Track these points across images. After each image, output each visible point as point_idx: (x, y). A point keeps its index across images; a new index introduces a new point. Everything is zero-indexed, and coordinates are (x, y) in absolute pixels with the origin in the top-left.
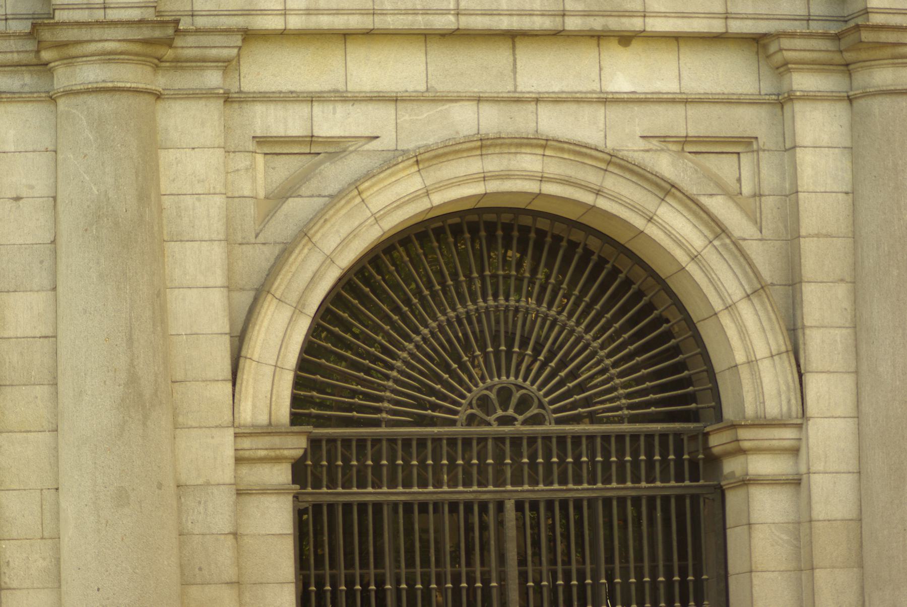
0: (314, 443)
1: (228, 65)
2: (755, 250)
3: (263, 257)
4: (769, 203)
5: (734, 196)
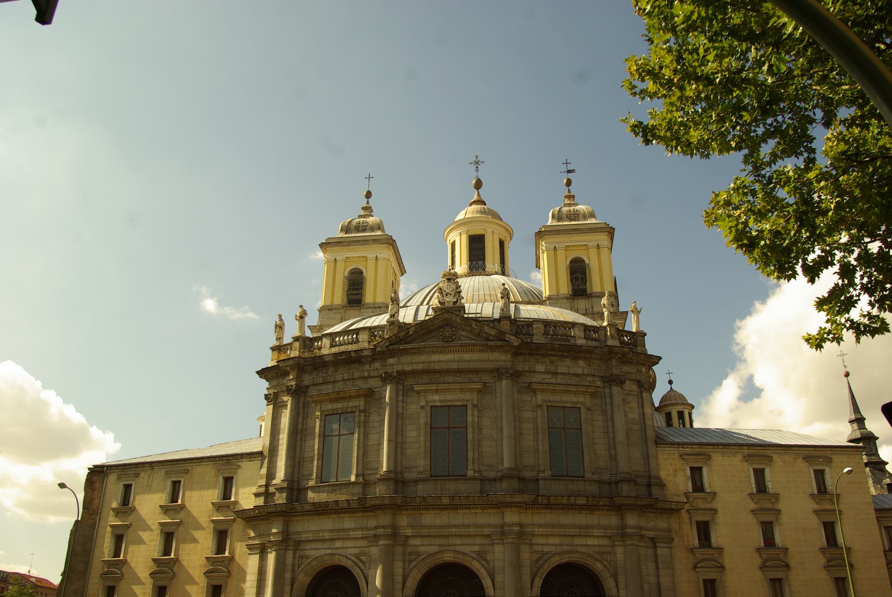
5: (607, 561)
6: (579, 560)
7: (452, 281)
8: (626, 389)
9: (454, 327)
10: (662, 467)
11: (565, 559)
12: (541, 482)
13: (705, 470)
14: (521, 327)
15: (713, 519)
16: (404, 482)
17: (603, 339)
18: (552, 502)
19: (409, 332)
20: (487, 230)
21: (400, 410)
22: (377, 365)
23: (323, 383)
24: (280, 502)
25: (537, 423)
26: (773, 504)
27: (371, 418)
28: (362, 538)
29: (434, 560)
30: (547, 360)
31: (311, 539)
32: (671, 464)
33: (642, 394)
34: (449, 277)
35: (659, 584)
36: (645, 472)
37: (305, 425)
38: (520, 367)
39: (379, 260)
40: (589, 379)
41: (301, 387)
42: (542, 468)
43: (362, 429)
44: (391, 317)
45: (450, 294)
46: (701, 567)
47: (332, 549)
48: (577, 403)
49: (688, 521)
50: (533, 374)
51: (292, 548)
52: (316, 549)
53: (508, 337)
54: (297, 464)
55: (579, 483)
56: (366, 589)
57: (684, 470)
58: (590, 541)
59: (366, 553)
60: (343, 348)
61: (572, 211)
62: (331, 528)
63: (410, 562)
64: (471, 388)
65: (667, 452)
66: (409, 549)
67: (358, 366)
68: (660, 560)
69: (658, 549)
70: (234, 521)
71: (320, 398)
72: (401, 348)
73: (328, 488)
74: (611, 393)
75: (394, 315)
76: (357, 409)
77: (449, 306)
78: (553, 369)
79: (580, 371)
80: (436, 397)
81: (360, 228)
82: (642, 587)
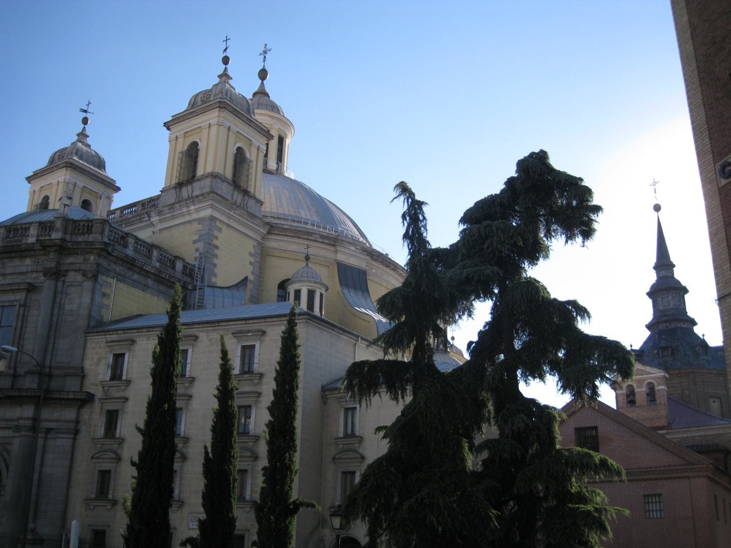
8: (68, 280)
13: (127, 356)
26: (187, 388)
32: (96, 353)
39: (60, 184)
48: (13, 301)
79: (24, 269)
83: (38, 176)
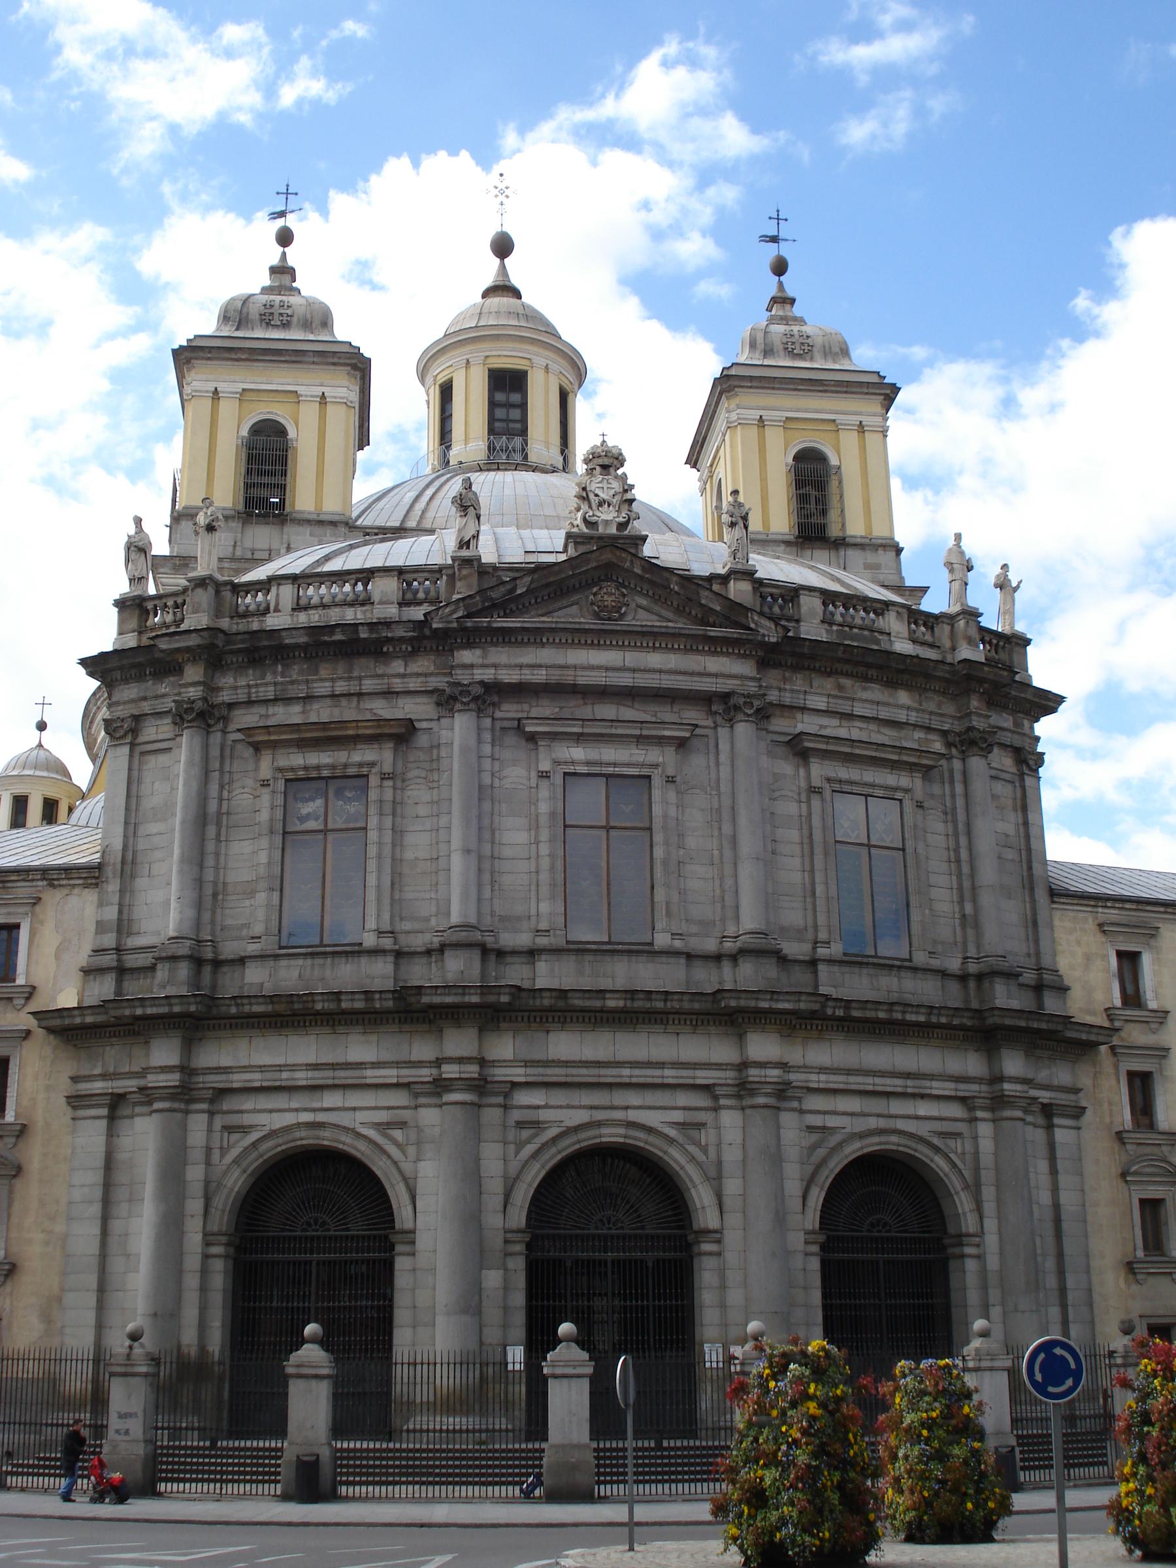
0: (828, 1237)
1: (800, 1099)
2: (966, 1173)
3: (810, 1169)
4: (968, 1157)
5: (956, 1153)
6: (901, 1149)
7: (612, 470)
9: (625, 587)
10: (1060, 948)
11: (873, 1145)
12: (821, 967)
13: (1146, 960)
14: (769, 599)
15: (1161, 1070)
16: (501, 954)
17: (947, 644)
18: (856, 1014)
19: (514, 589)
20: (536, 359)
21: (487, 780)
22: (423, 664)
23: (275, 700)
24: (171, 991)
25: (811, 828)
27: (409, 793)
28: (397, 1085)
29: (579, 1142)
30: (828, 684)
31: (257, 1084)
32: (1078, 943)
33: (1022, 780)
34: (606, 461)
35: (1056, 1206)
36: (1029, 955)
37: (225, 803)
38: (773, 696)
39: (329, 408)
40: (919, 734)
41: (213, 706)
42: (823, 936)
43: (388, 822)
44: (461, 547)
45: (609, 505)
46: (1136, 1173)
47: (314, 1110)
48: (896, 789)
49: (1111, 1070)
50: (799, 716)
51: (204, 1106)
52: (271, 1111)
53: (754, 620)
54: (208, 900)
55: (903, 974)
56: (410, 1208)
57: (1105, 957)
58: (924, 1109)
59: (406, 1123)
60: (334, 616)
61: (797, 337)
62: (312, 1059)
63: (520, 1146)
64: (664, 737)
65: (1071, 914)
66: (516, 1115)
67: (372, 665)
68: (1059, 1154)
69: (1056, 1130)
70: (28, 1033)
71: (272, 738)
72: (495, 625)
73: (300, 962)
74: (965, 773)
75: (468, 543)
76: (374, 770)
77: (608, 532)
78: (845, 707)
79: (902, 716)
80: (578, 753)
81: (267, 318)
82: (1031, 1212)
83: (234, 356)
